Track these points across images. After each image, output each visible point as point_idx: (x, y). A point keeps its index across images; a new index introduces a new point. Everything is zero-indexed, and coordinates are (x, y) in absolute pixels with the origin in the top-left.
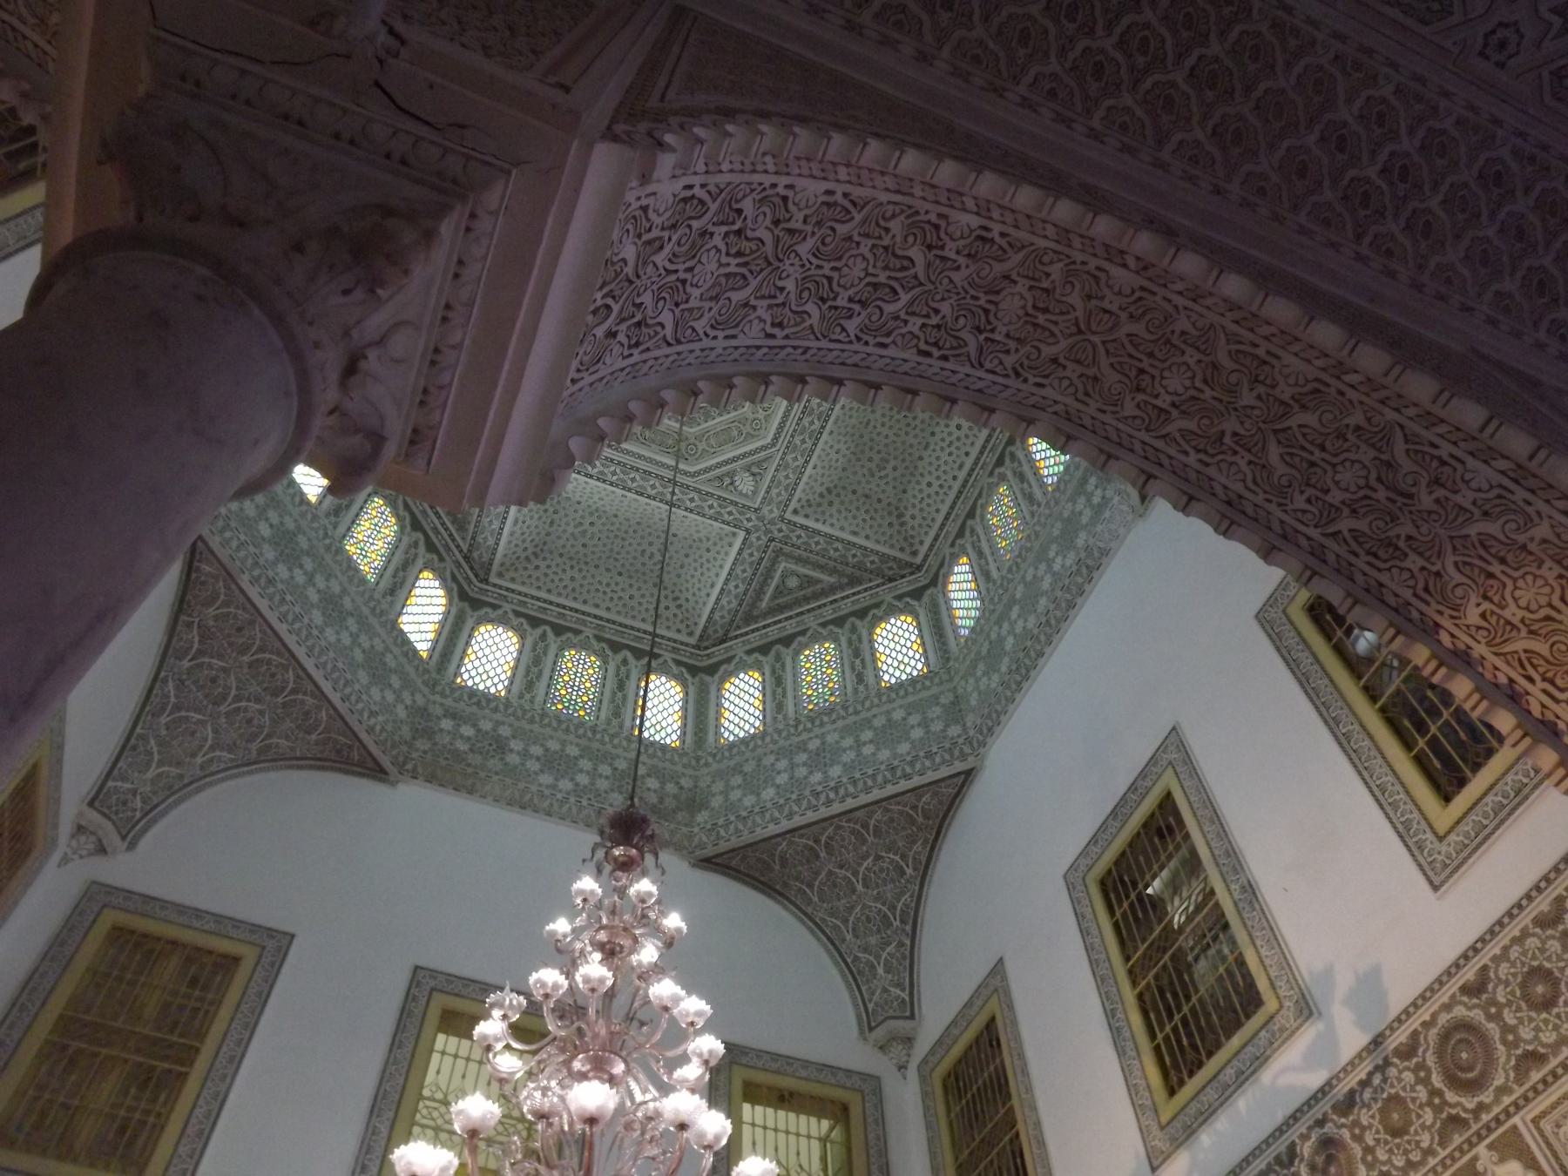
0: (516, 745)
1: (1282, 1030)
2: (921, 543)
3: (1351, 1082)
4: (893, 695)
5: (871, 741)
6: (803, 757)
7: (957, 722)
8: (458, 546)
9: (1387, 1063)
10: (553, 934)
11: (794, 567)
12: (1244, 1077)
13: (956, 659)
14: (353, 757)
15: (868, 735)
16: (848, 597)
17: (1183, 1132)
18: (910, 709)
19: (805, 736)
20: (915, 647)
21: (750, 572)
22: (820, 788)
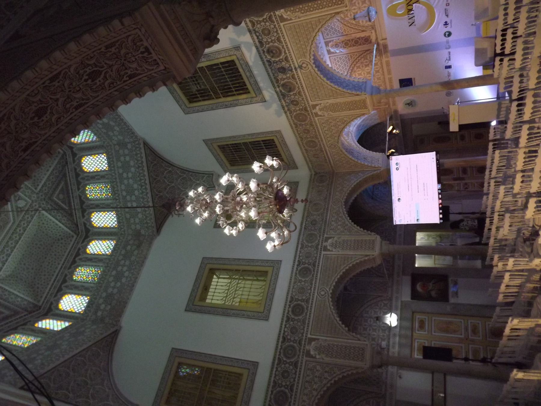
0: (110, 290)
1: (241, 56)
3: (257, 41)
5: (127, 174)
7: (127, 145)
8: (25, 315)
9: (254, 30)
10: (200, 223)
11: (56, 195)
13: (104, 142)
14: (110, 341)
15: (125, 175)
17: (259, 91)
19: (121, 197)
20: (95, 157)
22: (140, 191)
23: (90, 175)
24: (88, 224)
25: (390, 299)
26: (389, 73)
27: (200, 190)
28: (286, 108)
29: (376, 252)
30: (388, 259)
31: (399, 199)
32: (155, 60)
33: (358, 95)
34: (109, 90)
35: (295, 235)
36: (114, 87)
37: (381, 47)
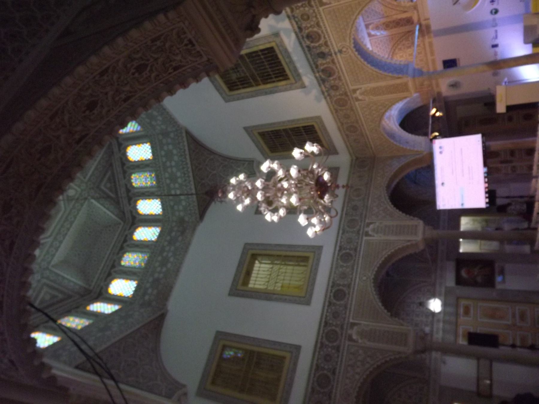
0: (156, 275)
3: (296, 26)
5: (171, 162)
12: (289, 56)
14: (157, 323)
15: (168, 164)
17: (298, 77)
22: (184, 179)
25: (434, 285)
26: (432, 53)
27: (242, 177)
28: (326, 94)
29: (419, 237)
30: (432, 245)
31: (443, 184)
32: (198, 52)
33: (399, 78)
34: (155, 82)
35: (337, 220)
36: (160, 79)
37: (424, 28)
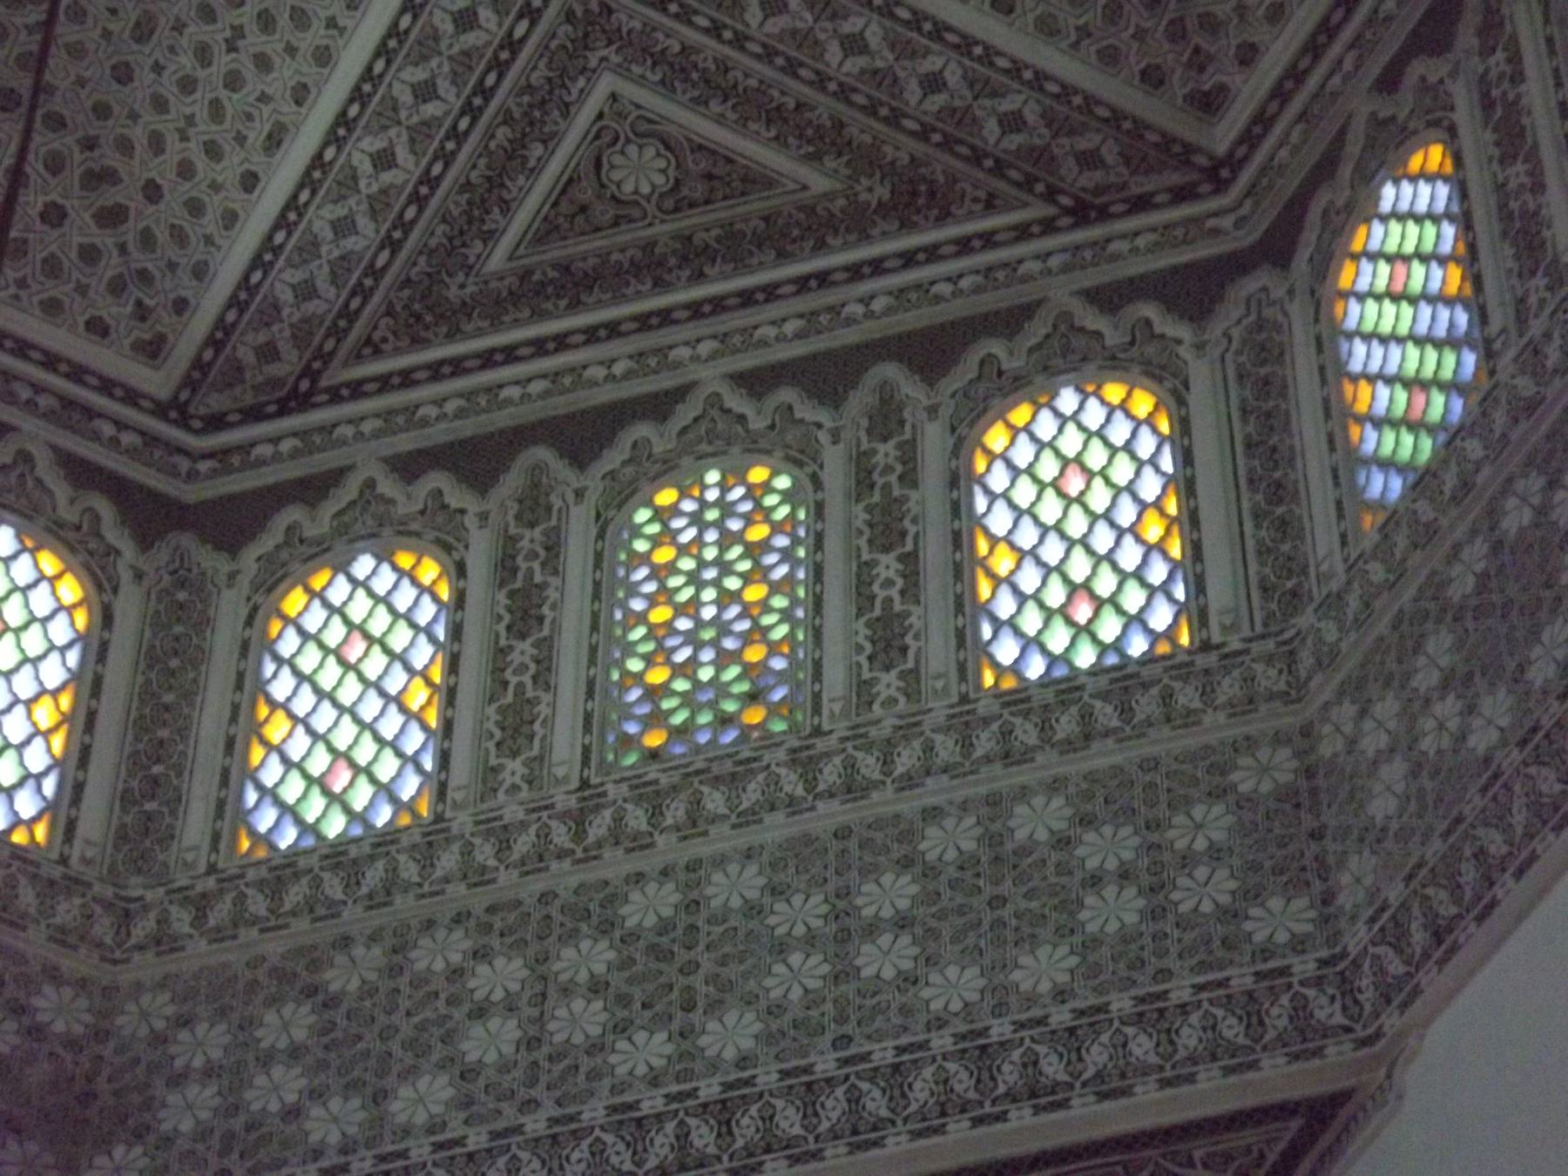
2: (1248, 55)
4: (1026, 733)
5: (902, 923)
6: (598, 956)
15: (890, 893)
16: (877, 267)
18: (1098, 802)
19: (615, 865)
20: (1153, 529)
21: (451, 96)
22: (652, 1103)
23: (930, 496)
24: (319, 522)
